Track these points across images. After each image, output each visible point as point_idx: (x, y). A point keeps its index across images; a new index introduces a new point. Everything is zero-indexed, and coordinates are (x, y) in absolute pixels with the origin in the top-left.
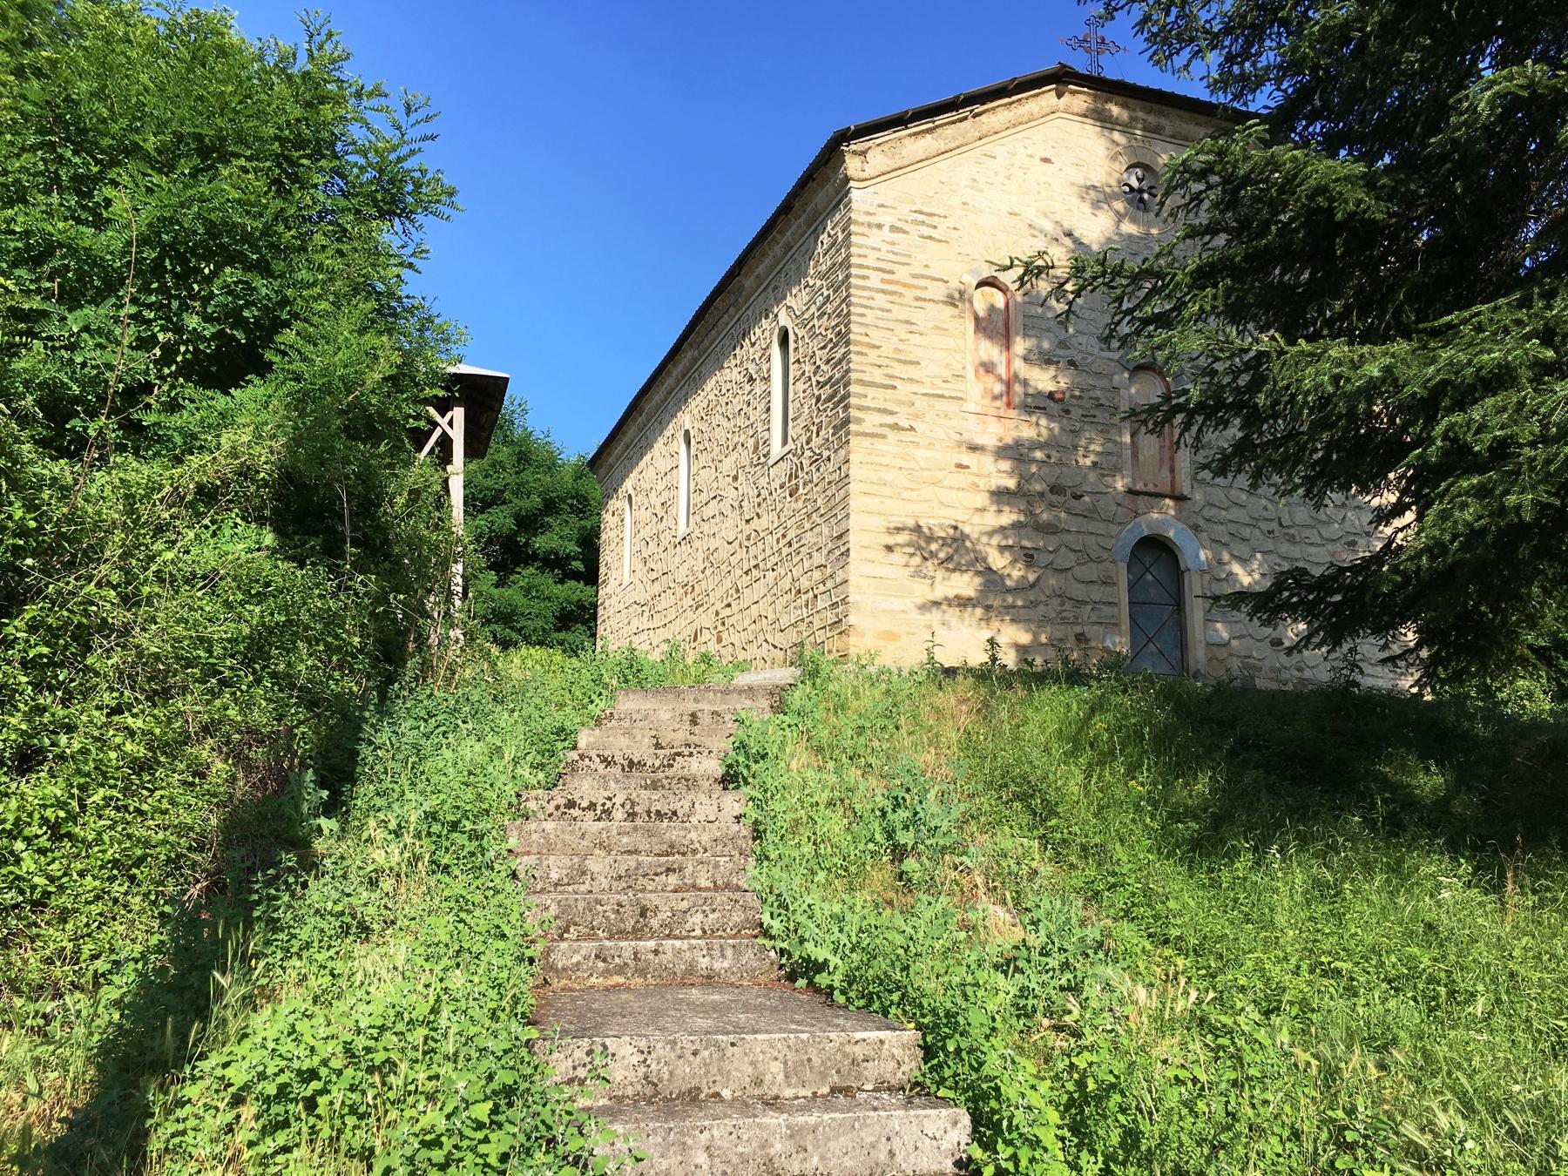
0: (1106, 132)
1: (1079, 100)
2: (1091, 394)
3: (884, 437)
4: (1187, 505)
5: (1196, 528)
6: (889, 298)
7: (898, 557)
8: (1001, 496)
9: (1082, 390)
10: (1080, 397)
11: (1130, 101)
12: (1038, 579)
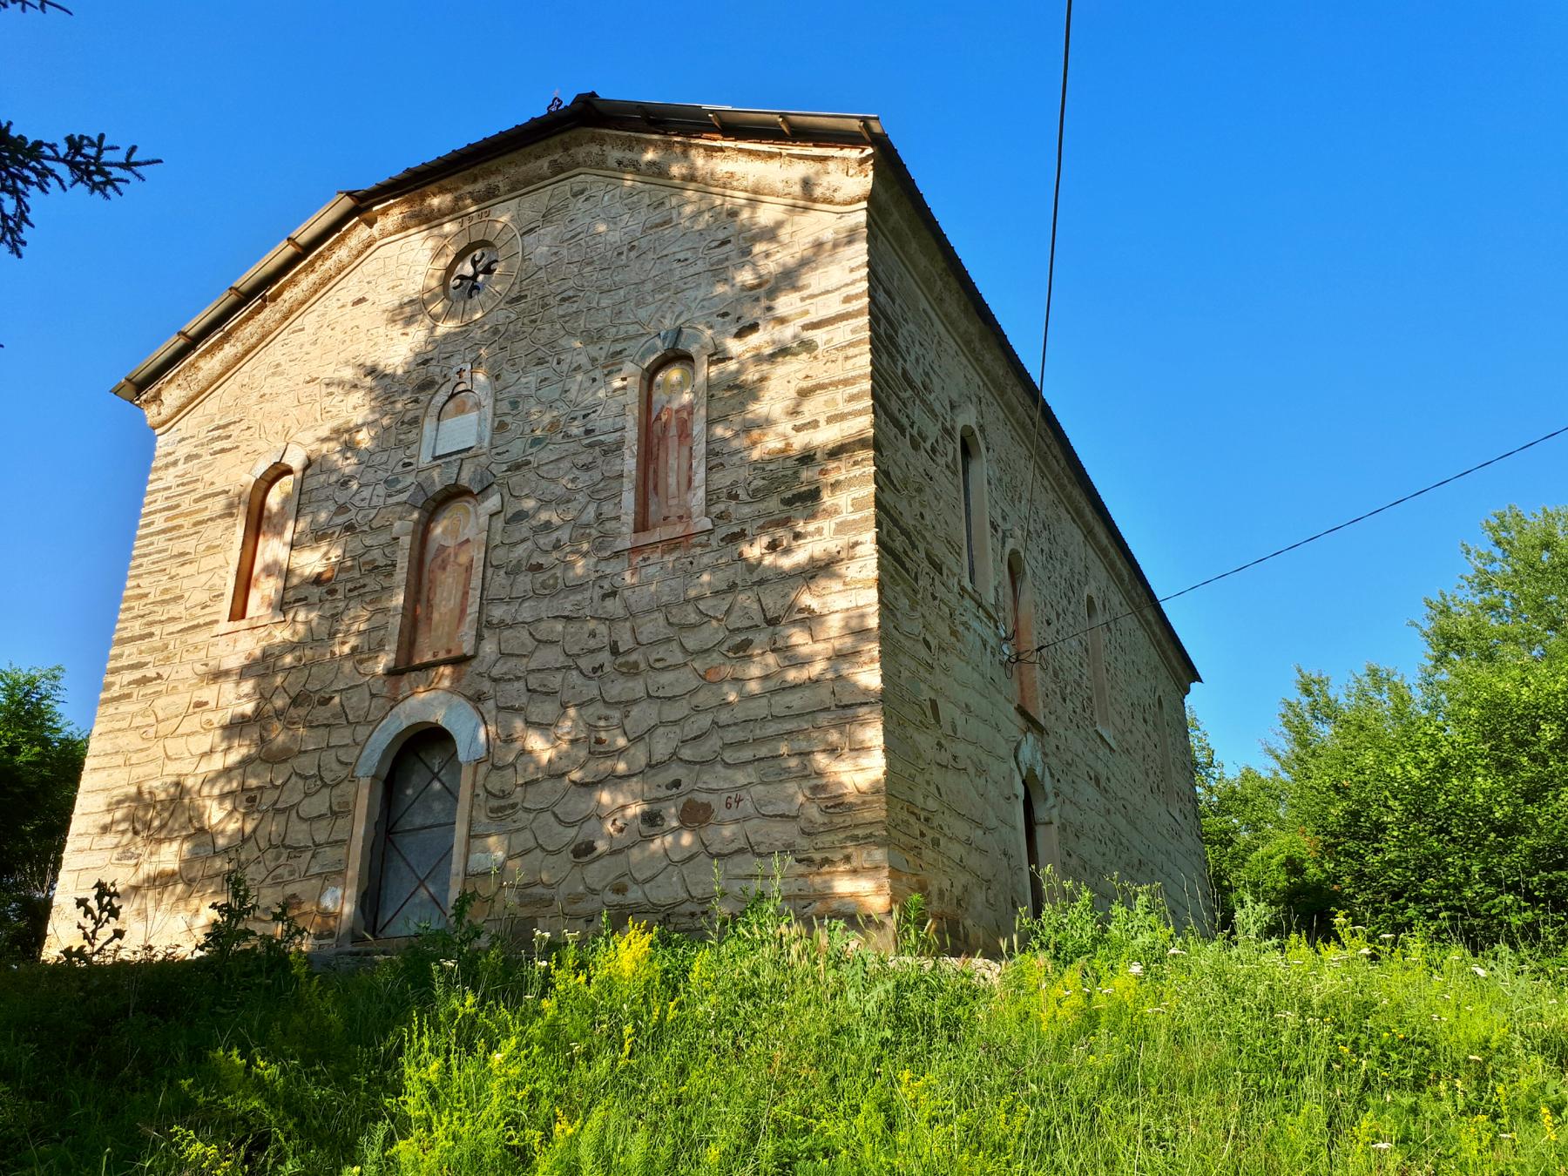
0: (435, 231)
1: (392, 215)
2: (368, 557)
3: (129, 696)
4: (467, 668)
5: (477, 699)
6: (169, 535)
7: (110, 839)
8: (235, 728)
9: (353, 558)
10: (352, 567)
11: (445, 182)
12: (254, 831)
